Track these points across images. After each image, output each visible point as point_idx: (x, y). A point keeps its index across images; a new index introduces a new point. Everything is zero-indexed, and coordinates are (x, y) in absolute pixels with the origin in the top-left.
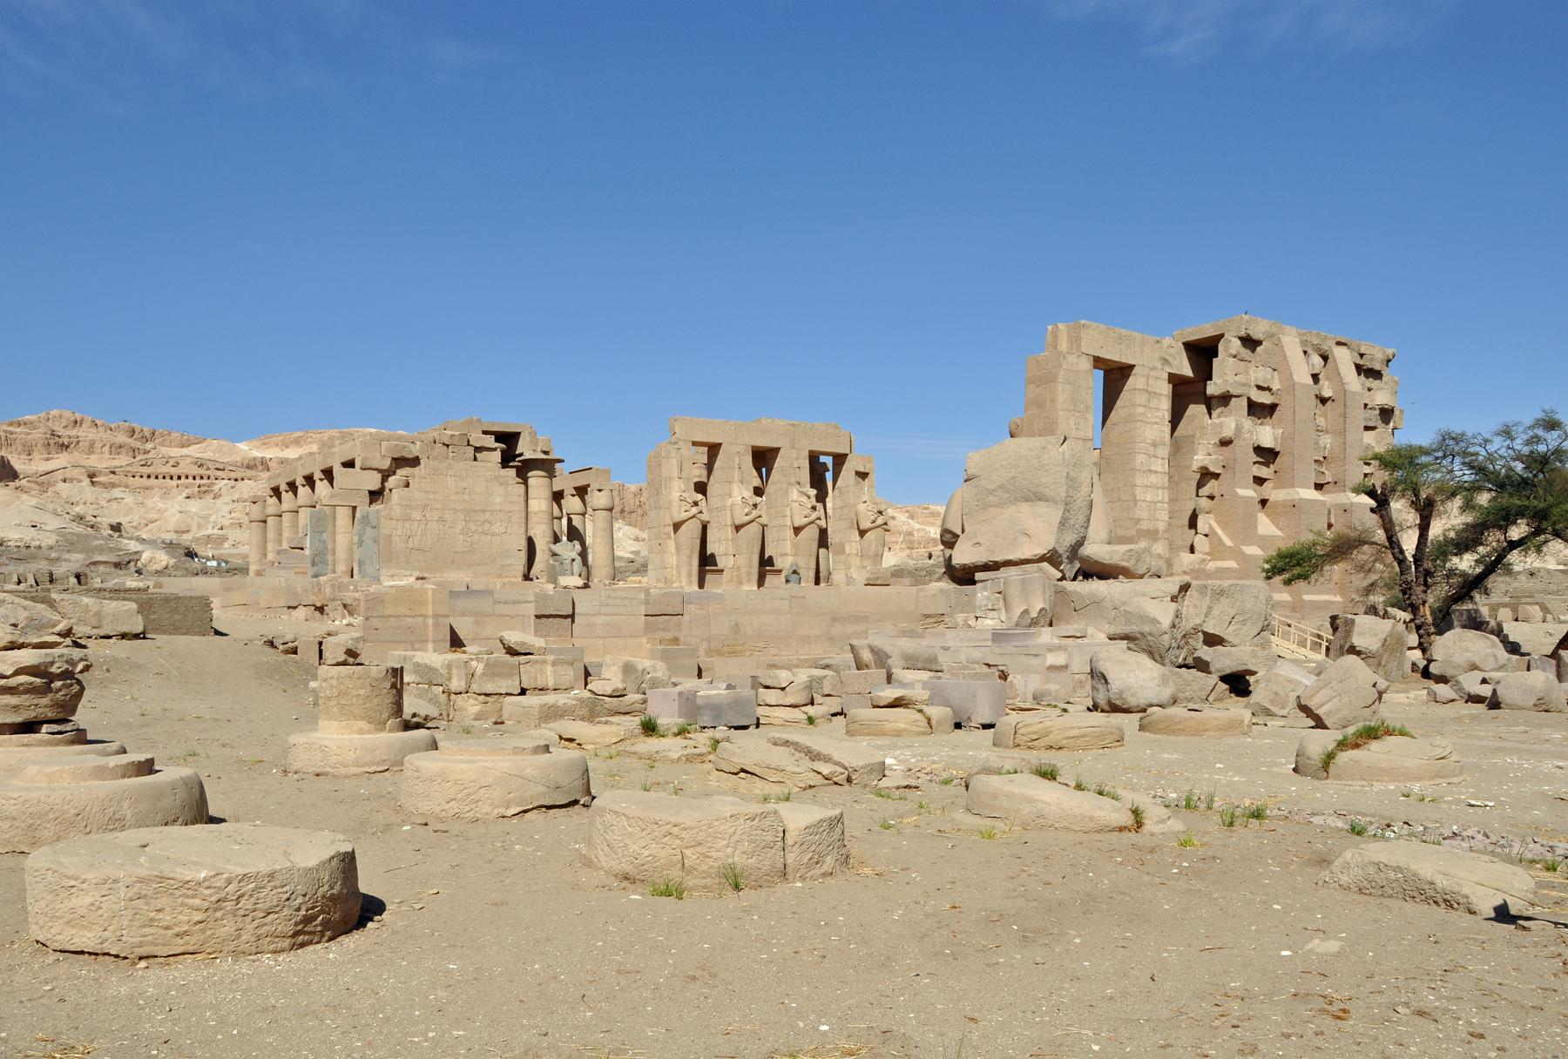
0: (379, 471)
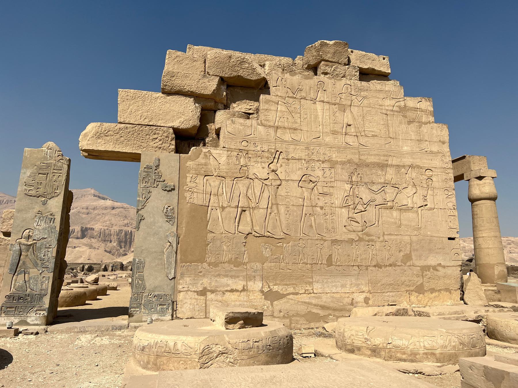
0: (197, 97)
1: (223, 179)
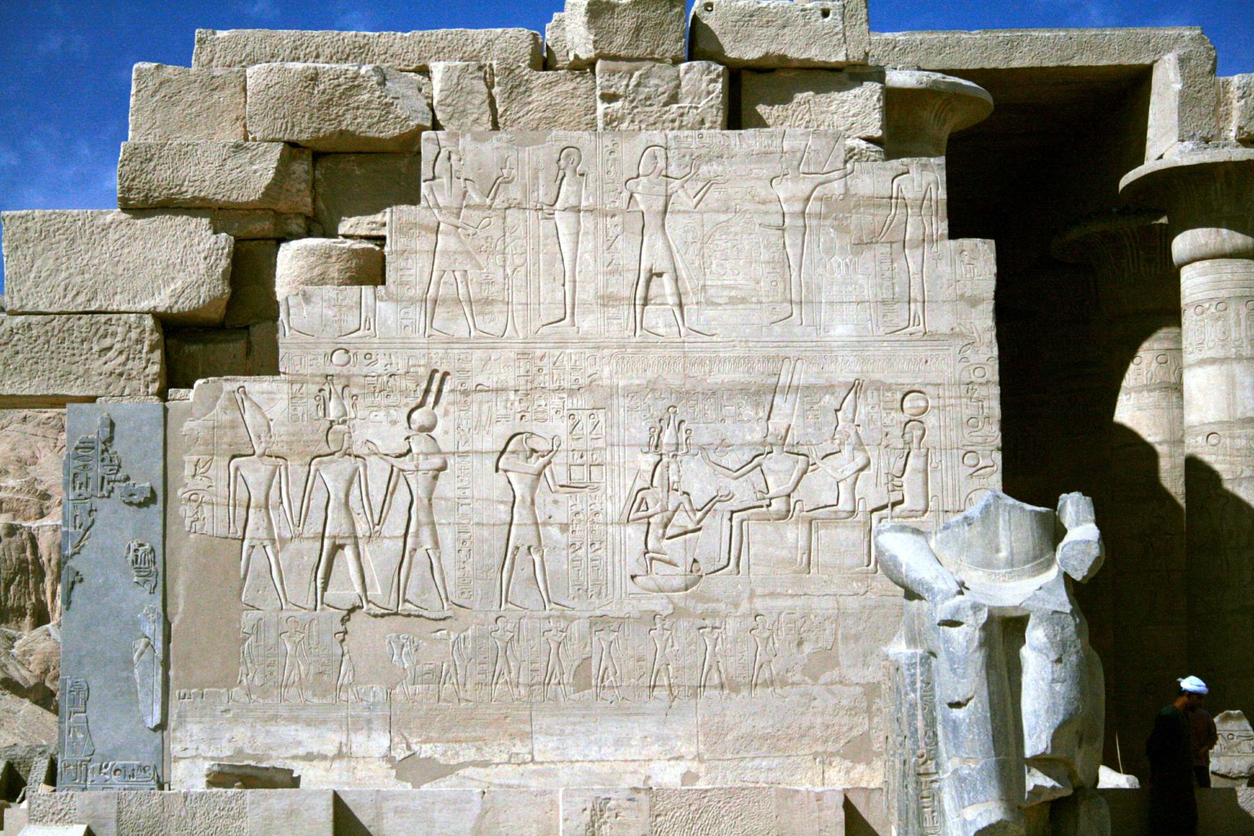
0: (218, 213)
1: (281, 461)
